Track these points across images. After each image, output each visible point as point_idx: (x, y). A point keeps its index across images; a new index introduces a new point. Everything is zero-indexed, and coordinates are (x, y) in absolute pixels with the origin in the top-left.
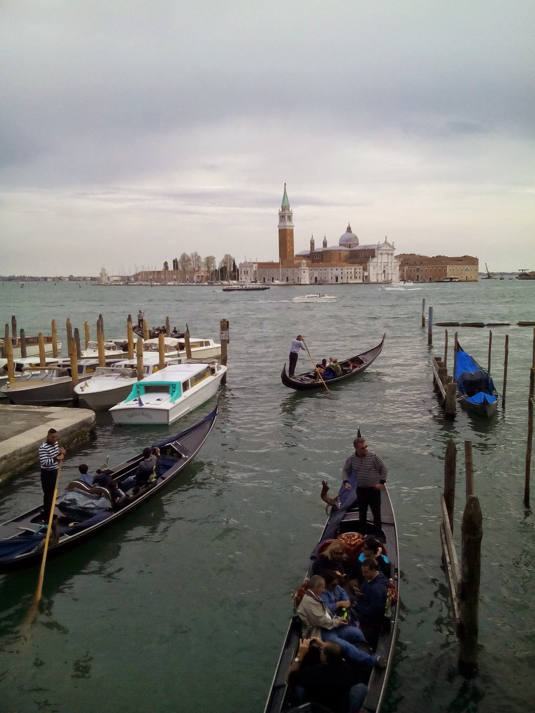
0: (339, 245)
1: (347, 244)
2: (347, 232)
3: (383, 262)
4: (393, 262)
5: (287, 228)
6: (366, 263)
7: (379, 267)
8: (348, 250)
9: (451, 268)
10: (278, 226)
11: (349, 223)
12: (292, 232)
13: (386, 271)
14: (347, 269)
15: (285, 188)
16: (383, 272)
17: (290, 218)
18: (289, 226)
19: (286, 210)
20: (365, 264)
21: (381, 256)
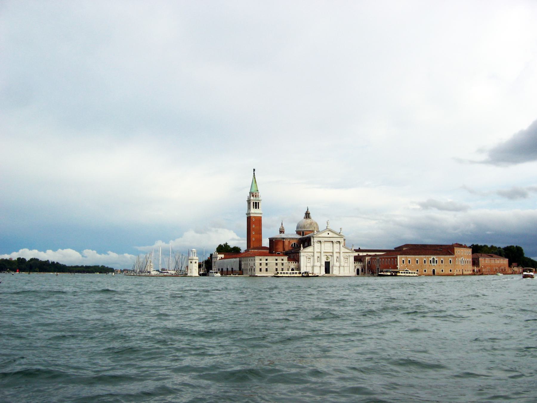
0: (296, 232)
1: (300, 231)
2: (304, 218)
3: (323, 251)
4: (341, 253)
5: (251, 215)
6: (299, 253)
7: (316, 257)
8: (296, 238)
9: (403, 259)
10: (247, 214)
11: (308, 208)
12: (259, 220)
13: (331, 262)
14: (261, 260)
15: (254, 173)
16: (324, 264)
17: (256, 205)
18: (256, 214)
19: (251, 197)
20: (298, 254)
21: (319, 244)
